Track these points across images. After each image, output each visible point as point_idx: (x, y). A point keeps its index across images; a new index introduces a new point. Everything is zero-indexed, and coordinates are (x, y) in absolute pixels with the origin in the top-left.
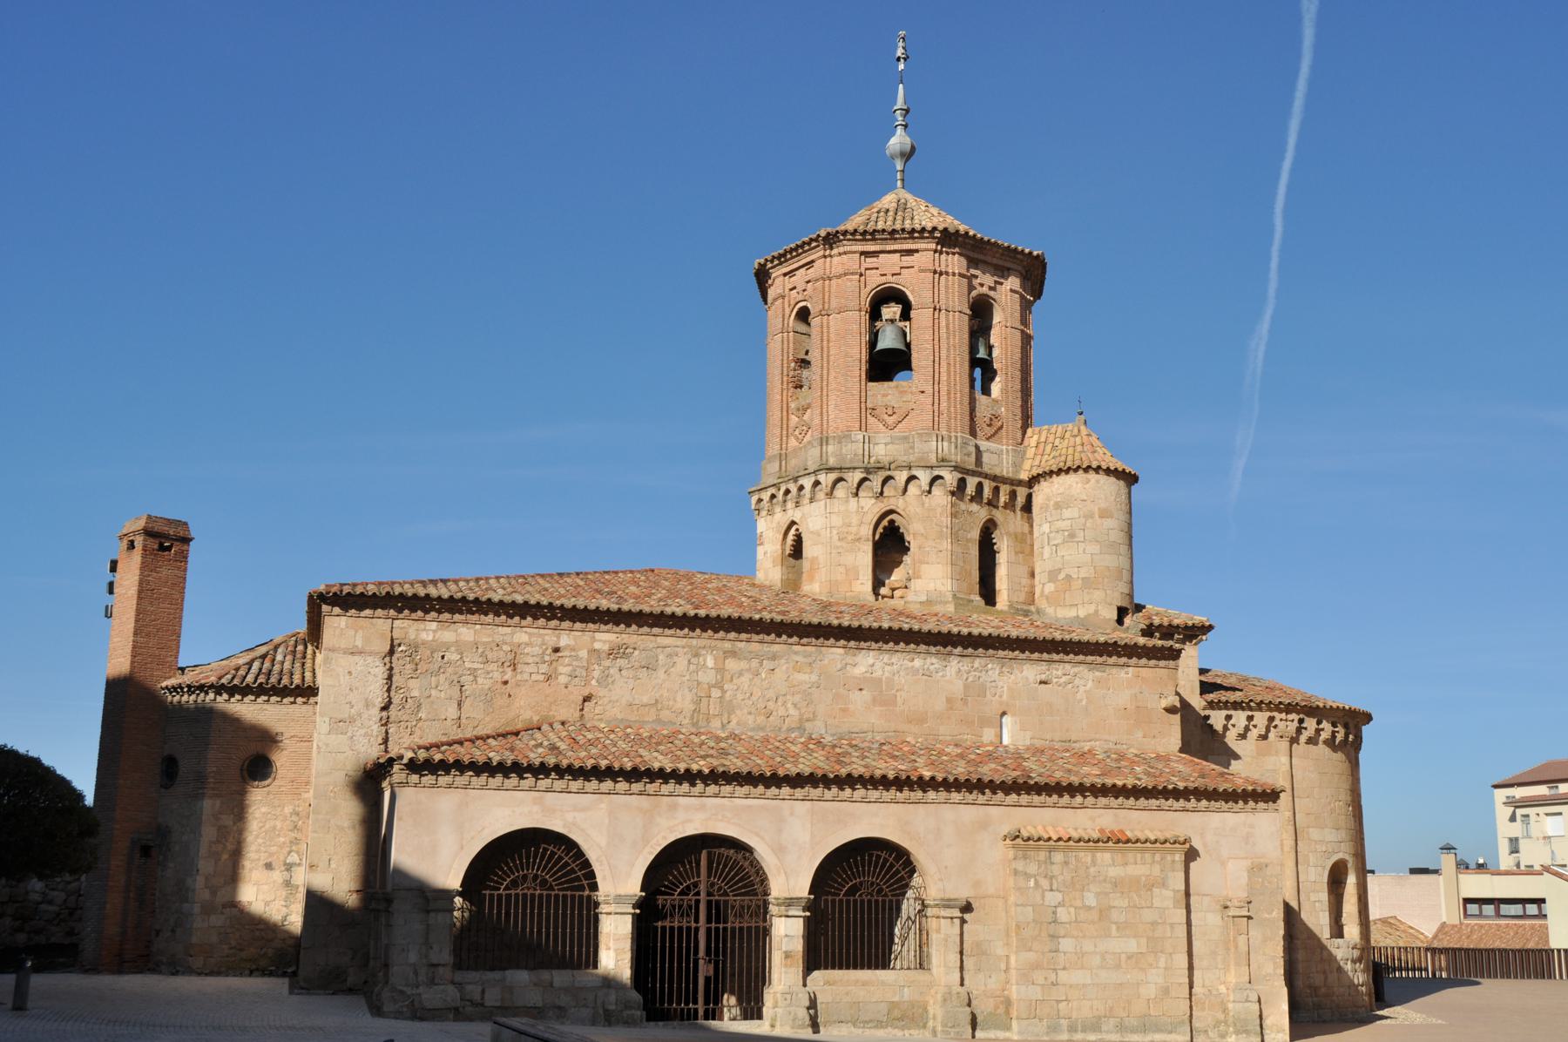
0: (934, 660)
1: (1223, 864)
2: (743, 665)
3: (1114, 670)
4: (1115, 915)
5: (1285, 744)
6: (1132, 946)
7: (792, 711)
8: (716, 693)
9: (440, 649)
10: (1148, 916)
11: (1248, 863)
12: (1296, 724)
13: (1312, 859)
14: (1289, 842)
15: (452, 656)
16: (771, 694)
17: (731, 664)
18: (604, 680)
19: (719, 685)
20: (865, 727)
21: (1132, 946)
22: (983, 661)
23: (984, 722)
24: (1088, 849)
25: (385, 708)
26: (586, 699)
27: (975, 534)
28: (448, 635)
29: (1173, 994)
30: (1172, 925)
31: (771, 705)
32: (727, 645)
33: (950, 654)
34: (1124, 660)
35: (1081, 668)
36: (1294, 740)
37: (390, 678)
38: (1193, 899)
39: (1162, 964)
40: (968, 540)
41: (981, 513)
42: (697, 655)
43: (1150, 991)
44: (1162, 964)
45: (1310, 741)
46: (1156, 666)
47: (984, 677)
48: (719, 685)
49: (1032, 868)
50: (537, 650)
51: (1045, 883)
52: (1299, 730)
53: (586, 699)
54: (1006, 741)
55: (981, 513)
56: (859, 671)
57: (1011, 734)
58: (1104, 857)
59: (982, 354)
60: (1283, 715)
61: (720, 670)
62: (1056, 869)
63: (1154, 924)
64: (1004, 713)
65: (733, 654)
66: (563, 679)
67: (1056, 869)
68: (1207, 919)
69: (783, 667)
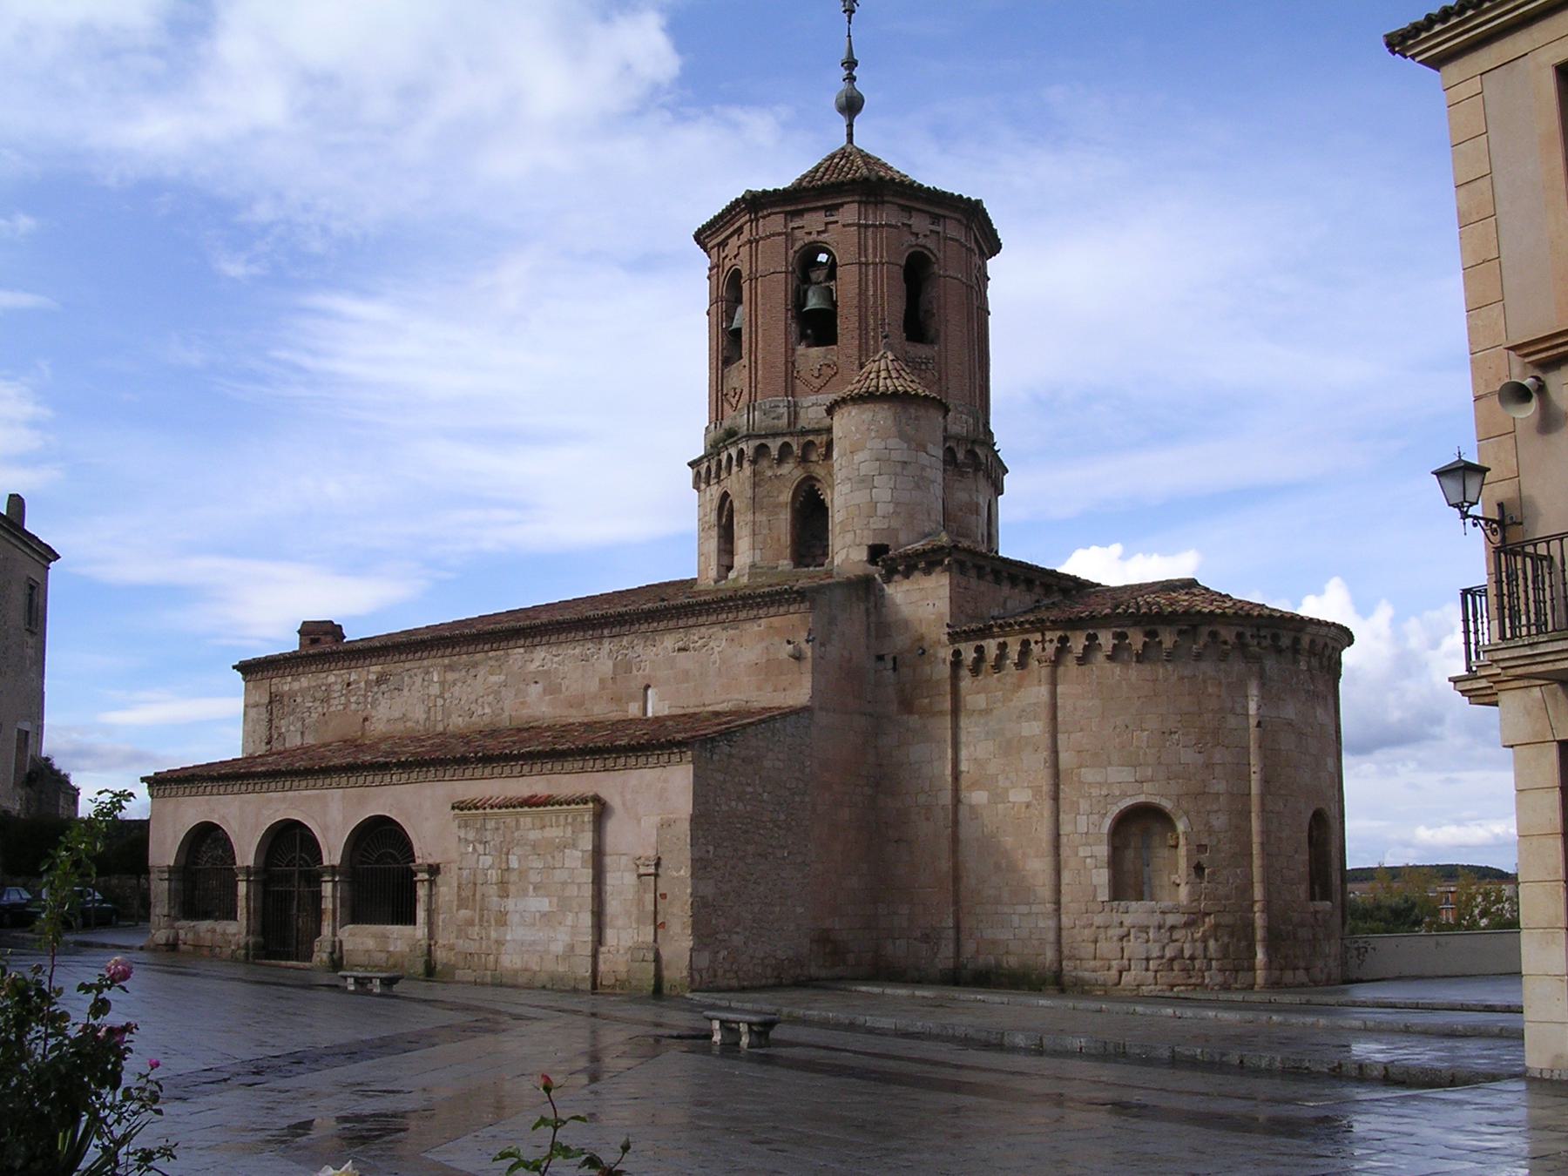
0: (590, 645)
1: (639, 821)
2: (456, 675)
3: (747, 626)
4: (534, 877)
5: (1045, 672)
6: (543, 904)
7: (487, 710)
8: (440, 702)
9: (292, 695)
10: (560, 875)
11: (656, 820)
12: (1056, 644)
13: (1084, 805)
14: (1046, 788)
15: (299, 700)
16: (473, 697)
17: (450, 676)
18: (374, 704)
19: (441, 696)
20: (538, 714)
21: (543, 904)
22: (629, 638)
23: (632, 698)
24: (511, 814)
25: (268, 743)
26: (366, 719)
27: (786, 496)
28: (296, 686)
29: (578, 951)
30: (579, 885)
31: (473, 707)
32: (446, 661)
33: (602, 637)
34: (753, 613)
35: (716, 629)
36: (1056, 662)
37: (270, 721)
38: (609, 861)
39: (569, 922)
40: (779, 505)
41: (791, 472)
42: (427, 673)
43: (558, 948)
44: (569, 922)
45: (1083, 660)
46: (788, 613)
47: (631, 654)
48: (441, 696)
49: (471, 836)
50: (338, 687)
51: (480, 848)
52: (1063, 648)
53: (366, 719)
54: (650, 714)
55: (791, 472)
56: (532, 667)
57: (656, 706)
58: (527, 818)
59: (813, 302)
60: (1038, 636)
61: (442, 683)
62: (488, 836)
63: (564, 883)
64: (647, 687)
65: (450, 668)
66: (353, 706)
67: (488, 836)
68: (620, 880)
69: (482, 671)
